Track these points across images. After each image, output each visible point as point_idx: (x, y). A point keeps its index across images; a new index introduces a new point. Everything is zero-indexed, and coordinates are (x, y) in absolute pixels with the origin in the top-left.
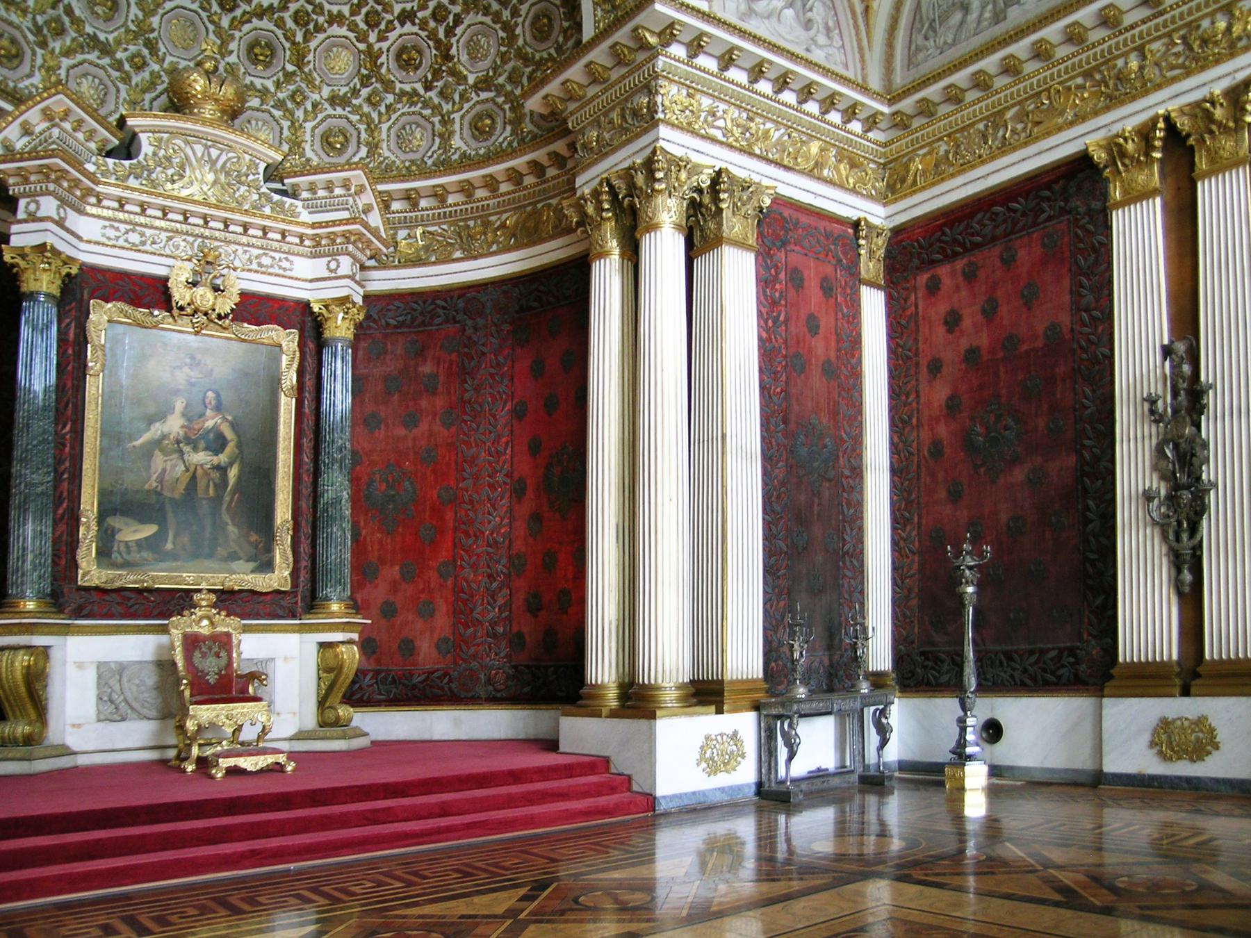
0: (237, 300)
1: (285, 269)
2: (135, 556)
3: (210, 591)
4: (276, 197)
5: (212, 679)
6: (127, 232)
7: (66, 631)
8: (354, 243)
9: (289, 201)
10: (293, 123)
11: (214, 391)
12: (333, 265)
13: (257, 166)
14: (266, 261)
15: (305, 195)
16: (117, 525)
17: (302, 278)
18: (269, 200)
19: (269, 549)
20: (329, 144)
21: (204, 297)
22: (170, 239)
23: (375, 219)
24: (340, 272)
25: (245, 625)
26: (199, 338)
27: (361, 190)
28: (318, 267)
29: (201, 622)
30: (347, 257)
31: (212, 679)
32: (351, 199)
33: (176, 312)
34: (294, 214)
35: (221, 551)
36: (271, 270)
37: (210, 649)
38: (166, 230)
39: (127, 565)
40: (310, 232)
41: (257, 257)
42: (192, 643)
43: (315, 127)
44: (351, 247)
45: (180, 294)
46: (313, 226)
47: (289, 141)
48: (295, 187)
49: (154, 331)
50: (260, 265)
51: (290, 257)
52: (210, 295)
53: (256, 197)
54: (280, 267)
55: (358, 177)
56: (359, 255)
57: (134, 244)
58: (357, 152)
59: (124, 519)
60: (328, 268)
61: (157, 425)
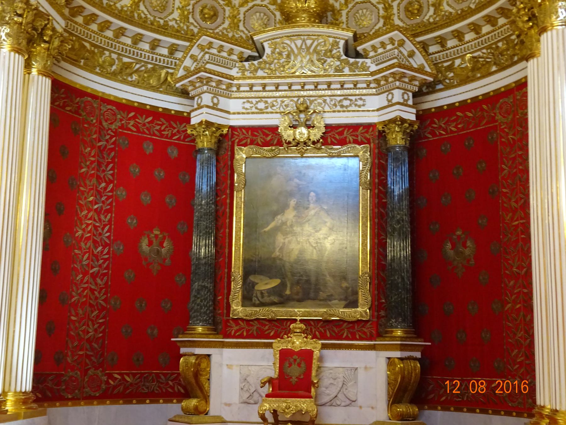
0: (324, 130)
1: (359, 106)
2: (267, 299)
3: (301, 321)
4: (352, 60)
5: (294, 380)
6: (257, 102)
7: (223, 345)
8: (399, 80)
9: (360, 60)
10: (385, 5)
11: (314, 191)
12: (390, 97)
13: (338, 43)
14: (346, 103)
15: (372, 54)
16: (256, 281)
17: (372, 109)
18: (347, 63)
19: (356, 293)
20: (410, 11)
21: (302, 133)
22: (283, 102)
23: (419, 60)
24: (394, 101)
25: (323, 344)
26: (303, 160)
27: (402, 44)
28: (381, 100)
29: (297, 342)
30: (397, 90)
31: (294, 380)
32: (396, 50)
33: (285, 145)
34: (365, 68)
35: (322, 295)
36: (349, 109)
37: (295, 360)
38: (280, 97)
39: (262, 305)
40: (371, 78)
41: (340, 101)
42: (285, 355)
43: (399, 4)
44: (398, 83)
45: (287, 134)
46: (372, 74)
47: (383, 17)
48: (365, 50)
49: (276, 160)
50: (342, 106)
51: (363, 97)
52: (304, 130)
53: (338, 63)
54: (356, 105)
55: (396, 35)
56: (409, 87)
57: (261, 110)
58: (428, 13)
59: (262, 277)
60: (388, 100)
61: (279, 217)
